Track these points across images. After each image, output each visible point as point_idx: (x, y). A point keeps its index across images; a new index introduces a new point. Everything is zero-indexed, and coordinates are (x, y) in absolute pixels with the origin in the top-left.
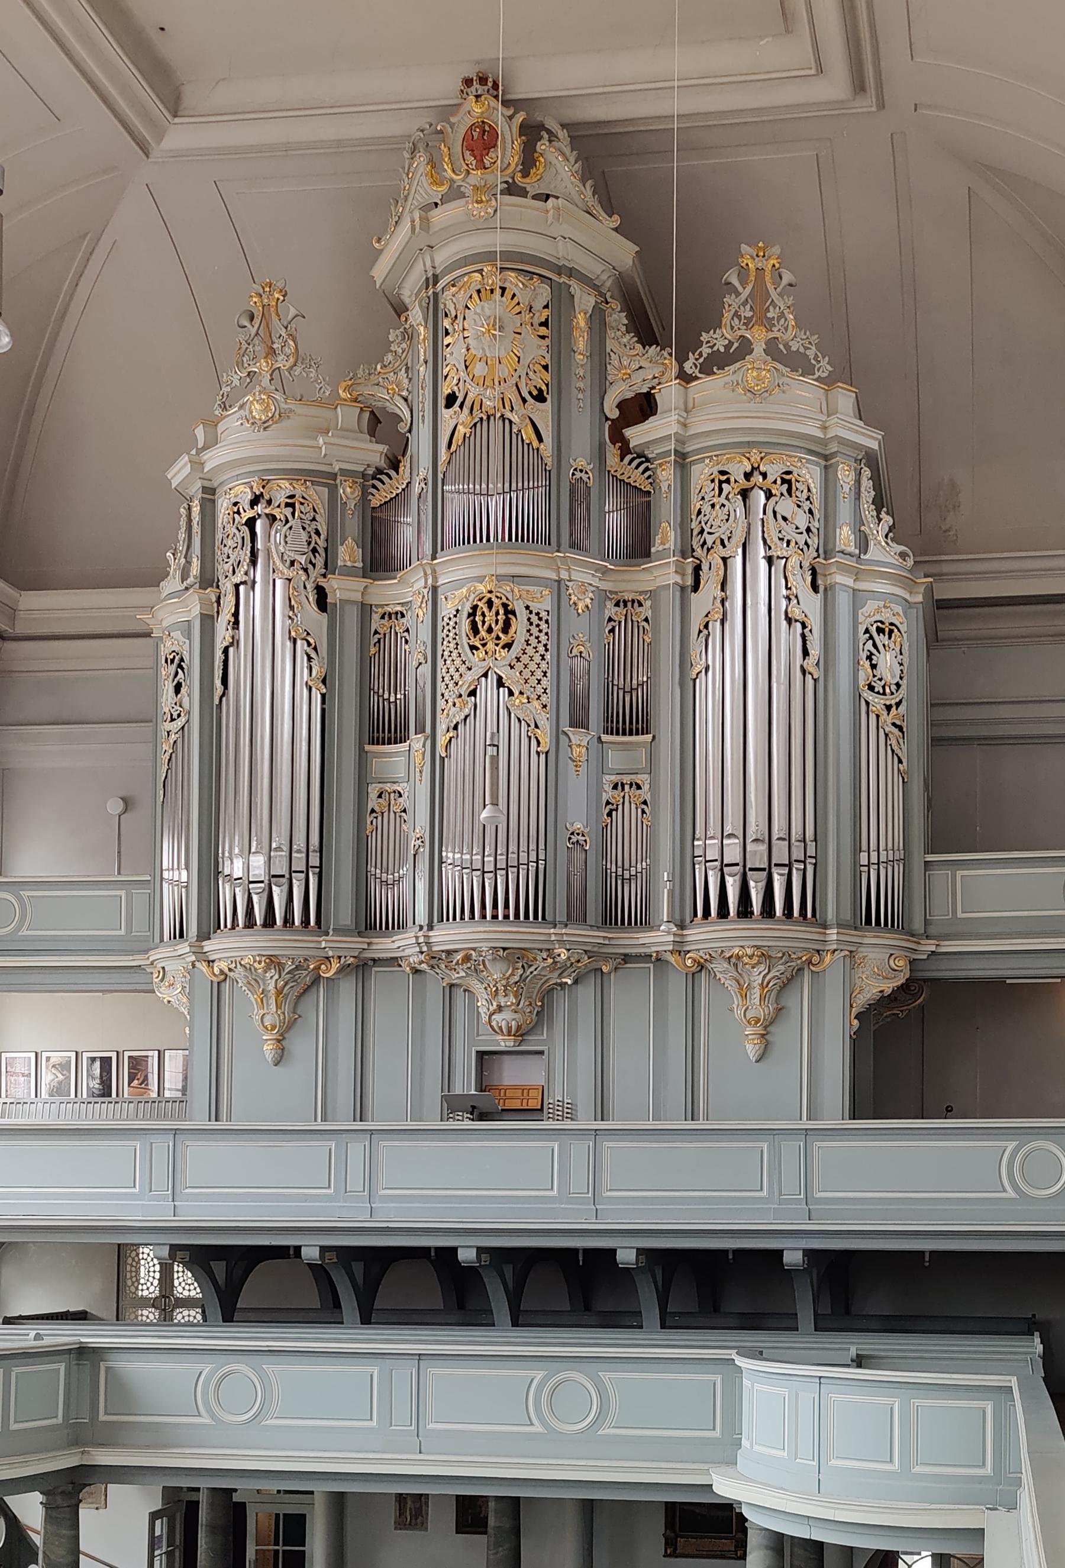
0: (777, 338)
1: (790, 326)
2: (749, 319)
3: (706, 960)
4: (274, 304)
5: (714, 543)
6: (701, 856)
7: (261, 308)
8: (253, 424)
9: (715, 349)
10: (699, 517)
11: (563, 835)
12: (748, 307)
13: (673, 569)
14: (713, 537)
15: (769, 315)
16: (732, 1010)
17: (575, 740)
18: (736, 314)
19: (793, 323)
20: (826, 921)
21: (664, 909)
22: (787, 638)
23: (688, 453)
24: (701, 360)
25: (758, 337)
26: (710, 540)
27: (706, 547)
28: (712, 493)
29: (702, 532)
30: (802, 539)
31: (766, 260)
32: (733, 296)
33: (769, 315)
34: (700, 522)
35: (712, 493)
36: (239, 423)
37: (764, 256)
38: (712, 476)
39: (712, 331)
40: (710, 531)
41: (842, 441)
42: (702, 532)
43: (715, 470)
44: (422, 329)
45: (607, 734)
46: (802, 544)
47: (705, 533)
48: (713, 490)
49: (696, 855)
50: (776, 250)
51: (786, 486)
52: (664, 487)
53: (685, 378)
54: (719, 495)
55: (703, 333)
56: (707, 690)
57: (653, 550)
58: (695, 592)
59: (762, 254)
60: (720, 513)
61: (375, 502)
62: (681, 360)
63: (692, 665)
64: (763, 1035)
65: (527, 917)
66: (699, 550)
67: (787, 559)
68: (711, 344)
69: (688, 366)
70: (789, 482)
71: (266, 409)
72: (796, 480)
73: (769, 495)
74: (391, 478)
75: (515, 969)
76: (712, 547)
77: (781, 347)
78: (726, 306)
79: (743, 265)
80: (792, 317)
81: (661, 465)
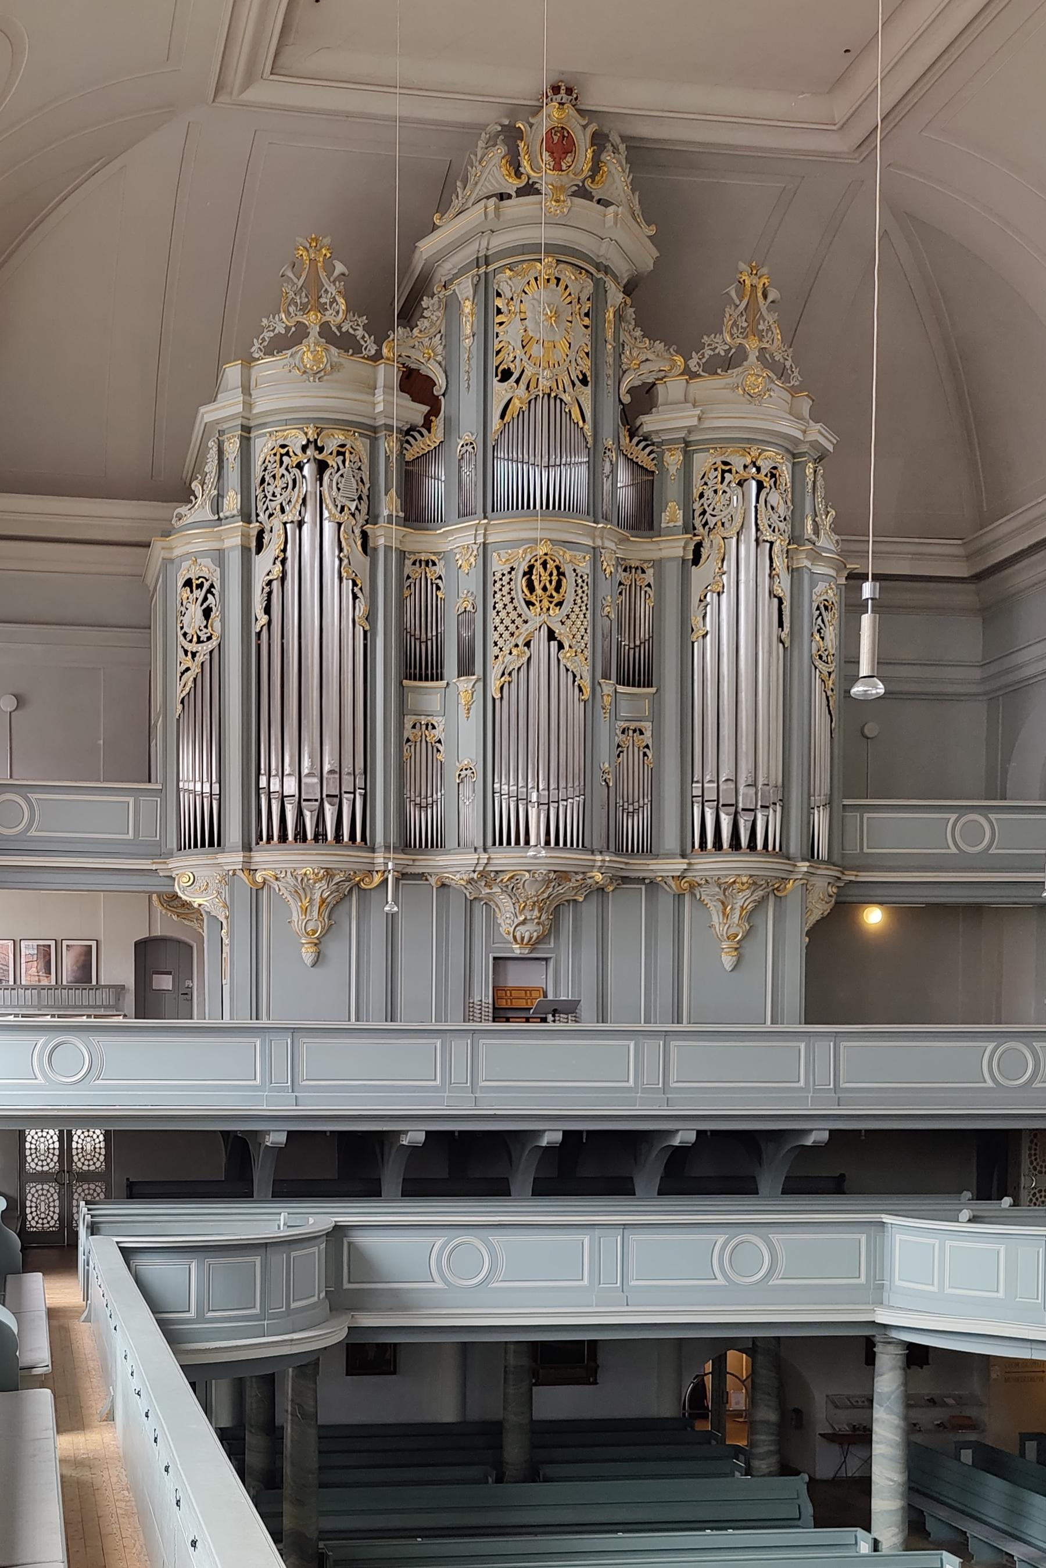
0: (765, 348)
1: (775, 340)
2: (745, 328)
3: (699, 885)
4: (321, 259)
5: (716, 524)
6: (699, 796)
7: (308, 262)
8: (305, 372)
9: (717, 351)
10: (702, 500)
11: (598, 774)
12: (744, 318)
13: (682, 544)
14: (714, 520)
15: (760, 327)
16: (711, 926)
17: (606, 692)
18: (735, 323)
19: (779, 337)
20: (788, 853)
21: (670, 840)
22: (768, 609)
23: (690, 441)
24: (704, 360)
25: (752, 346)
26: (712, 521)
27: (707, 527)
28: (715, 481)
29: (704, 513)
30: (782, 525)
31: (759, 278)
32: (733, 308)
33: (760, 327)
34: (702, 505)
35: (715, 481)
36: (287, 369)
37: (756, 274)
38: (716, 466)
39: (713, 335)
40: (713, 513)
41: (815, 444)
42: (704, 513)
43: (719, 461)
44: (468, 303)
45: (624, 685)
46: (782, 531)
47: (707, 515)
48: (716, 477)
49: (694, 794)
50: (764, 270)
51: (774, 479)
52: (673, 470)
53: (690, 375)
54: (722, 482)
55: (705, 337)
56: (705, 652)
57: (663, 525)
58: (696, 565)
59: (755, 272)
60: (719, 500)
61: (409, 457)
62: (687, 358)
63: (693, 630)
64: (736, 949)
65: (557, 843)
66: (701, 528)
67: (772, 543)
68: (713, 347)
69: (693, 363)
70: (773, 476)
71: (317, 360)
72: (780, 475)
73: (760, 486)
74: (422, 436)
75: (547, 887)
76: (714, 528)
77: (767, 356)
78: (727, 316)
79: (741, 280)
80: (778, 331)
81: (668, 449)
